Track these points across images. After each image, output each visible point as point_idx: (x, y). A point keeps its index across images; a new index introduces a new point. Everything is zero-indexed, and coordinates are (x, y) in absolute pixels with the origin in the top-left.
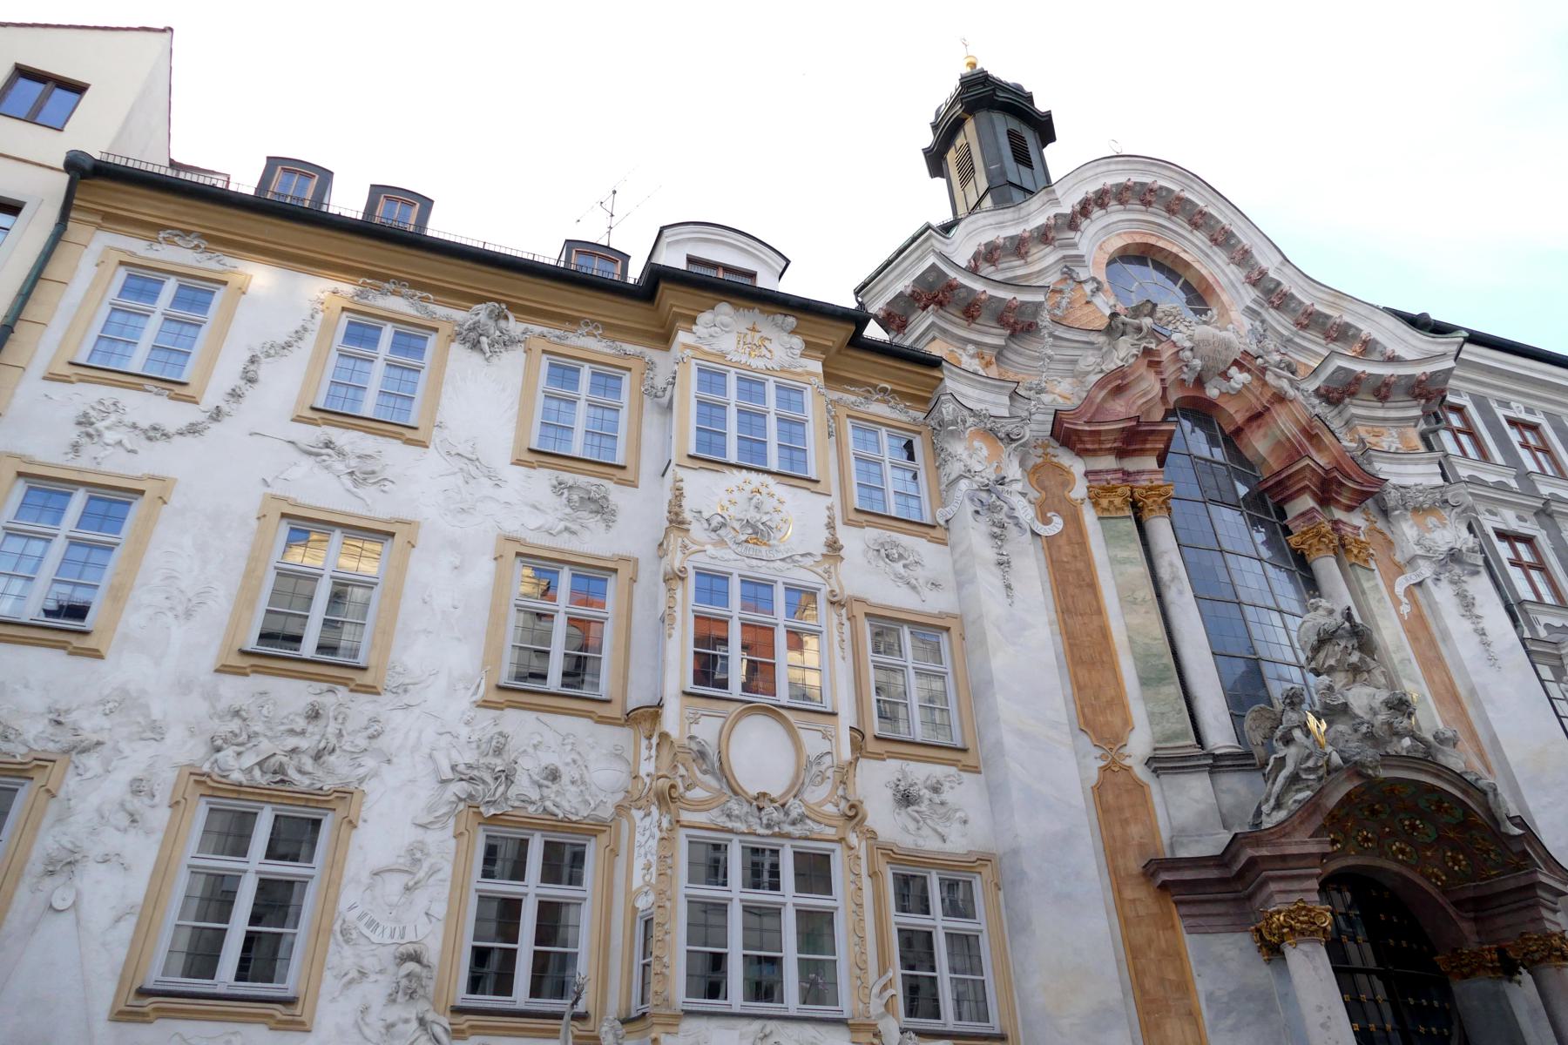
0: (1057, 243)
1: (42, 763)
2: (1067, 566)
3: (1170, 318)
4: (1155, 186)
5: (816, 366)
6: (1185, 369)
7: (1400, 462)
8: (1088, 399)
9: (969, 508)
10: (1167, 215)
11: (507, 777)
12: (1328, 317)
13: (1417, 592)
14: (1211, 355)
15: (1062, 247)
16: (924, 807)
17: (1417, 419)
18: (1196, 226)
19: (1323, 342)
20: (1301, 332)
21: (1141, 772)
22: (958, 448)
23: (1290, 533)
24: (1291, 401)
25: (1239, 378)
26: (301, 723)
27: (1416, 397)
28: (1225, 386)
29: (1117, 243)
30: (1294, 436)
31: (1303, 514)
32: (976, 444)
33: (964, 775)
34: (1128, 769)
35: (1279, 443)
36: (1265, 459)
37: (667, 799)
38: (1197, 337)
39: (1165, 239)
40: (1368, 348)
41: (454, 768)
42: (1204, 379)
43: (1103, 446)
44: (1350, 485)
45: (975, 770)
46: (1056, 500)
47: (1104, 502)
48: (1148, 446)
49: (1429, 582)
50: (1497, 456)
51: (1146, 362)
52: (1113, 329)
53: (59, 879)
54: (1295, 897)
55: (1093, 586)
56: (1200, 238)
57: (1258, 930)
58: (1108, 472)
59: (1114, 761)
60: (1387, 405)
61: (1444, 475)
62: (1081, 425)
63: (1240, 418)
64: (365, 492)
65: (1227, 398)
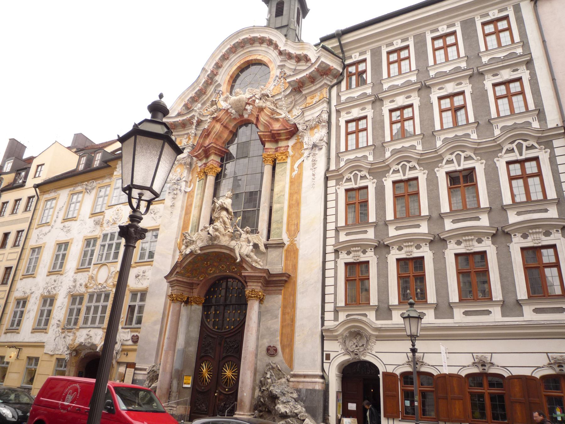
0: (213, 83)
4: (240, 41)
7: (314, 108)
10: (251, 46)
11: (75, 287)
14: (236, 106)
15: (215, 83)
16: (139, 277)
20: (298, 64)
25: (249, 107)
29: (234, 68)
32: (177, 169)
39: (252, 55)
42: (241, 114)
48: (210, 152)
51: (215, 121)
60: (315, 84)
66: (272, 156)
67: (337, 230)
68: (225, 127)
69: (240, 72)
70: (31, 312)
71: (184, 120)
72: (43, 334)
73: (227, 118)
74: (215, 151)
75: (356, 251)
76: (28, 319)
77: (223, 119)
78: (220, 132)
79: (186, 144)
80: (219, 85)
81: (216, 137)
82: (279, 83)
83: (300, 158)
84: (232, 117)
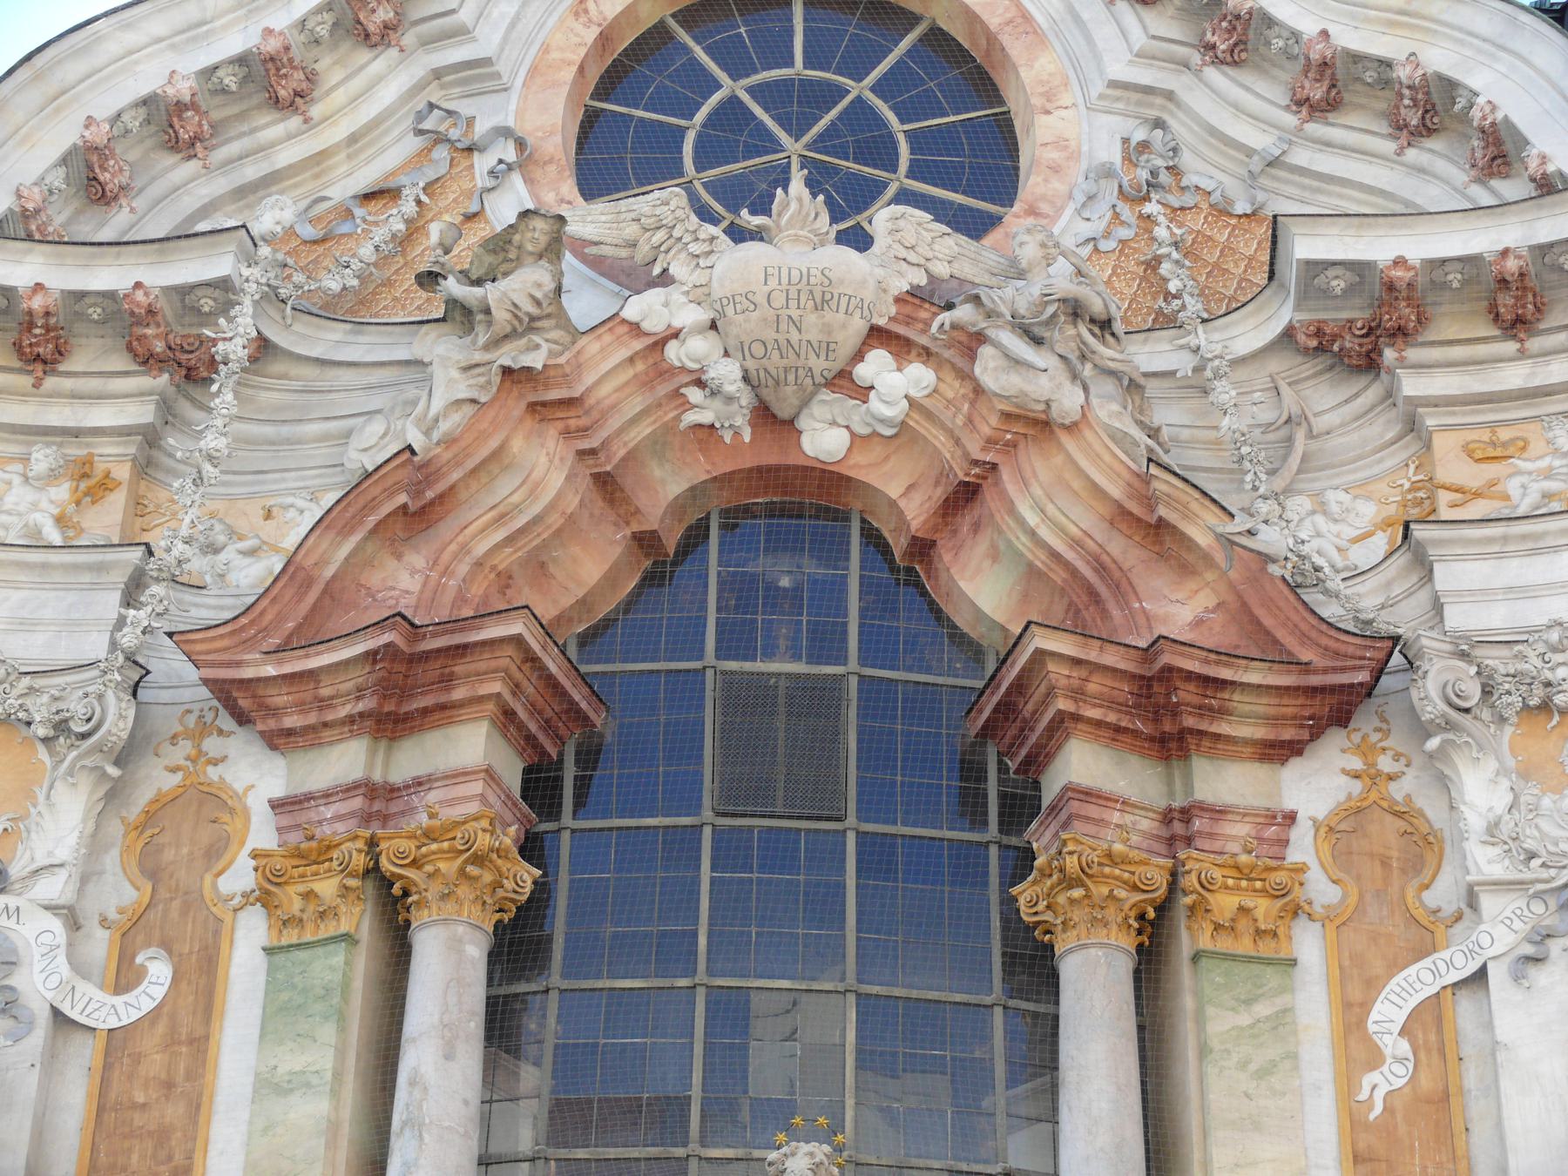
0: (409, 39)
2: (138, 1119)
3: (660, 236)
6: (695, 395)
7: (1536, 548)
8: (294, 572)
12: (1387, 64)
13: (1465, 1009)
14: (769, 335)
15: (427, 42)
19: (1389, 147)
20: (1313, 128)
24: (1071, 428)
28: (856, 415)
30: (1076, 543)
35: (1032, 573)
38: (718, 291)
42: (783, 412)
43: (330, 716)
44: (1254, 678)
46: (176, 904)
48: (459, 694)
49: (1496, 974)
58: (327, 796)
60: (1534, 344)
62: (256, 664)
63: (917, 511)
65: (877, 451)
66: (1139, 869)
68: (607, 485)
69: (674, 16)
71: (81, 295)
73: (644, 413)
74: (516, 689)
77: (604, 415)
78: (555, 520)
79: (55, 537)
81: (506, 559)
82: (1125, 233)
83: (1420, 953)
84: (691, 417)
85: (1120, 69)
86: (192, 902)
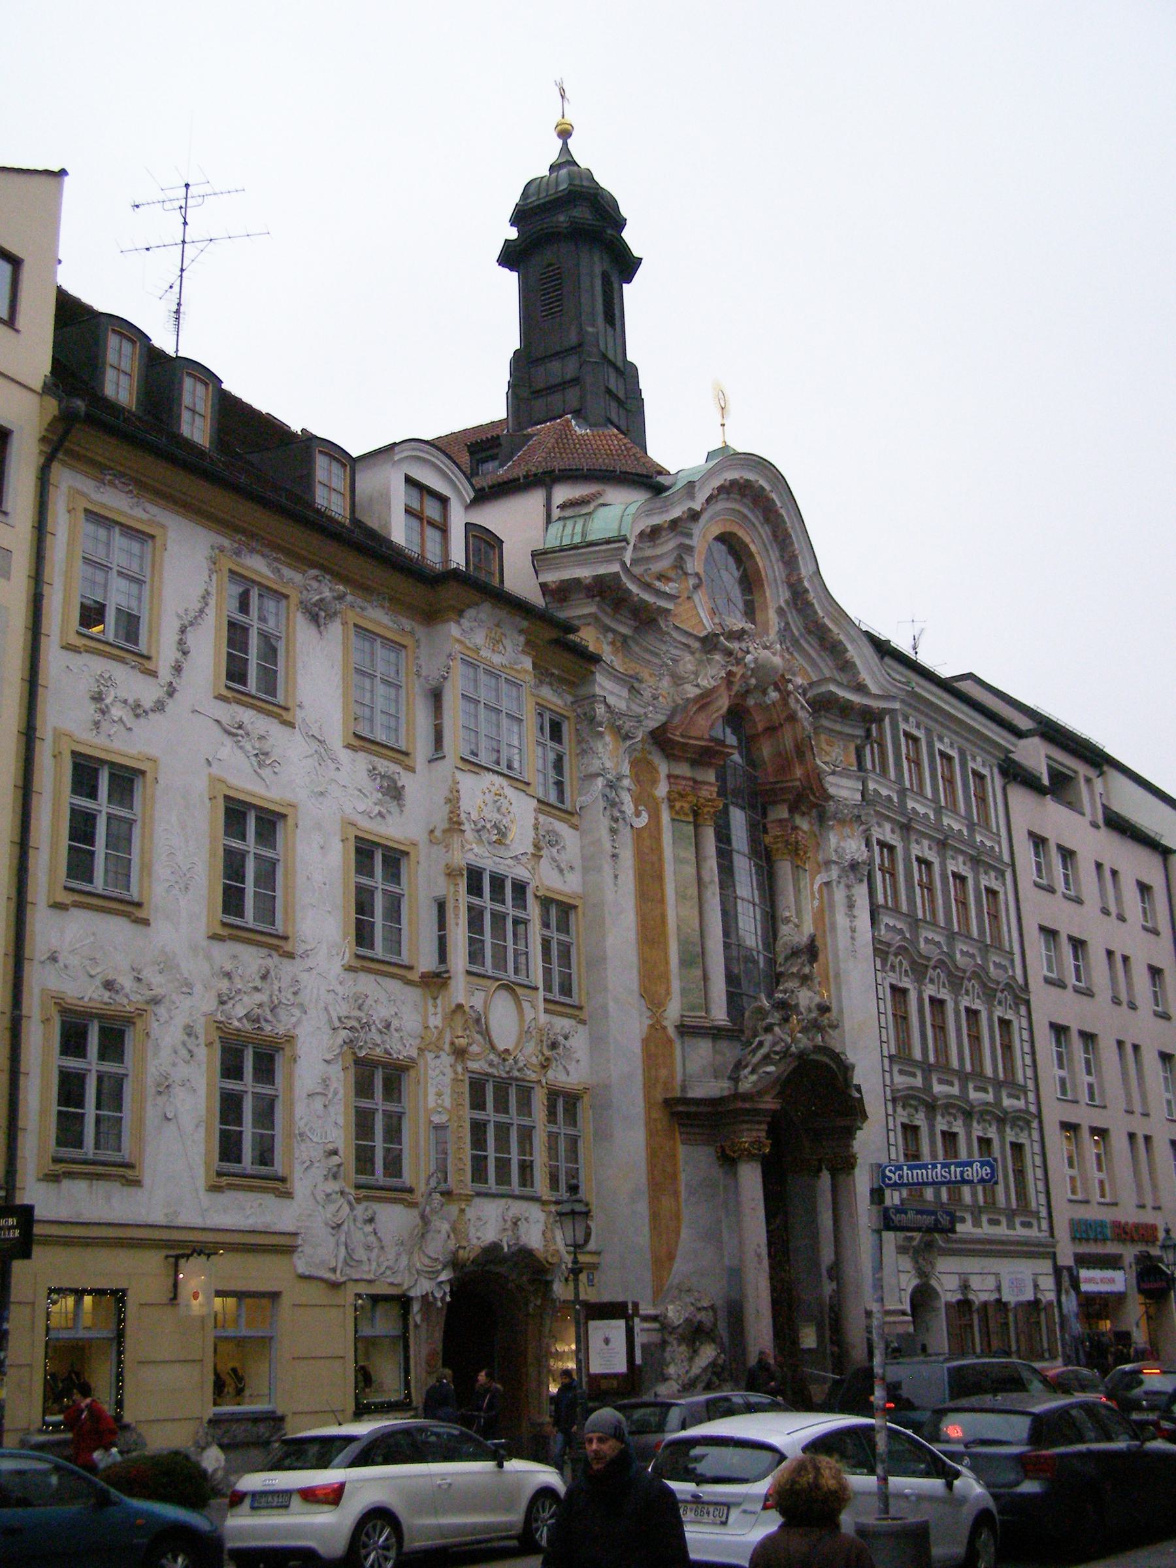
1: (140, 1013)
5: (527, 663)
9: (602, 804)
12: (830, 630)
13: (825, 889)
17: (857, 737)
18: (767, 520)
21: (671, 1031)
22: (599, 746)
23: (765, 831)
25: (774, 695)
26: (258, 983)
27: (864, 721)
29: (716, 531)
31: (781, 821)
33: (579, 1026)
34: (664, 1028)
35: (780, 754)
36: (765, 763)
37: (460, 1053)
40: (846, 666)
41: (340, 1019)
45: (583, 1022)
47: (678, 805)
48: (714, 761)
49: (834, 884)
50: (892, 774)
52: (709, 643)
53: (164, 1098)
54: (754, 1134)
55: (660, 878)
56: (765, 531)
57: (723, 1148)
58: (684, 778)
59: (658, 1021)
61: (863, 796)
63: (760, 727)
64: (266, 772)
67: (891, 1057)
70: (179, 1093)
72: (269, 1200)
75: (911, 1106)
76: (172, 1126)
80: (689, 549)
85: (783, 605)
86: (651, 796)
